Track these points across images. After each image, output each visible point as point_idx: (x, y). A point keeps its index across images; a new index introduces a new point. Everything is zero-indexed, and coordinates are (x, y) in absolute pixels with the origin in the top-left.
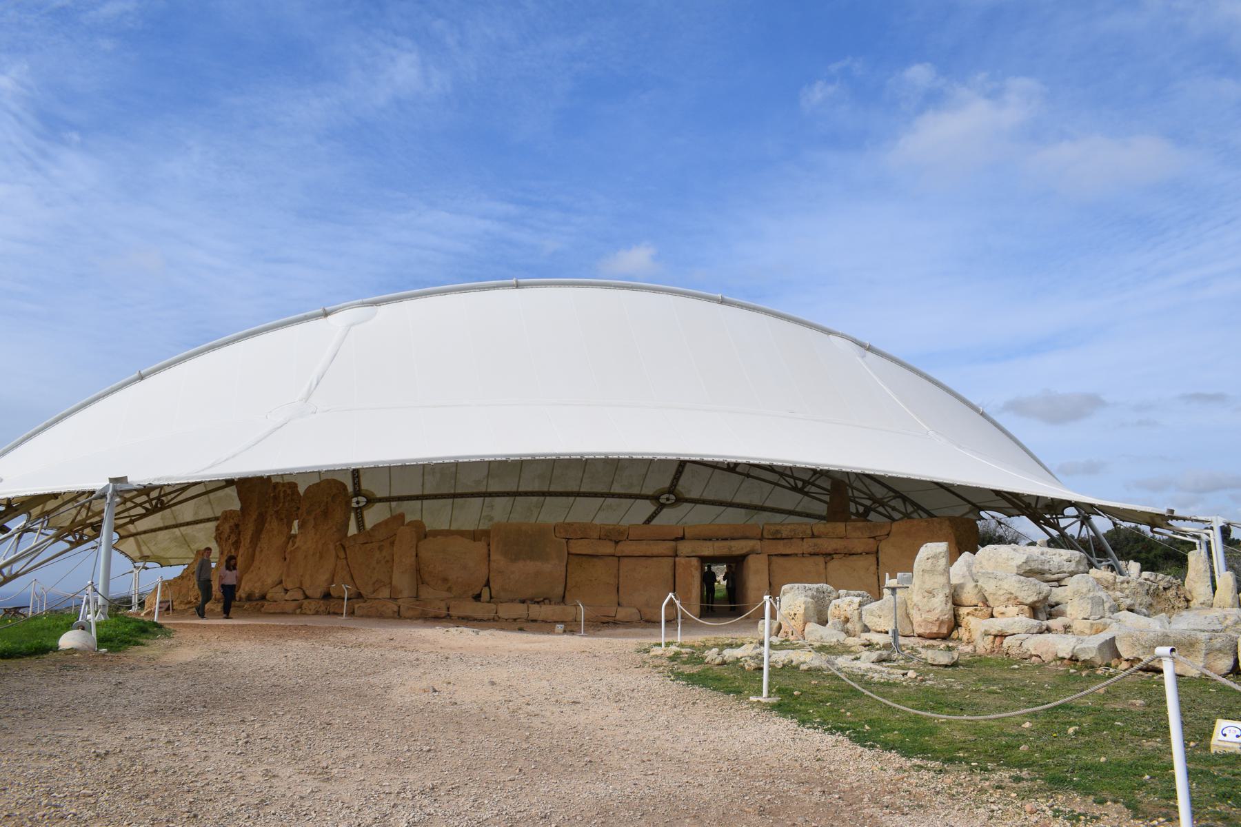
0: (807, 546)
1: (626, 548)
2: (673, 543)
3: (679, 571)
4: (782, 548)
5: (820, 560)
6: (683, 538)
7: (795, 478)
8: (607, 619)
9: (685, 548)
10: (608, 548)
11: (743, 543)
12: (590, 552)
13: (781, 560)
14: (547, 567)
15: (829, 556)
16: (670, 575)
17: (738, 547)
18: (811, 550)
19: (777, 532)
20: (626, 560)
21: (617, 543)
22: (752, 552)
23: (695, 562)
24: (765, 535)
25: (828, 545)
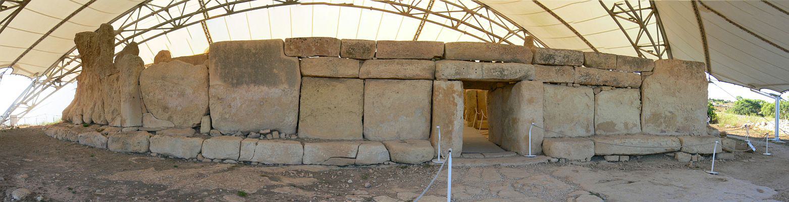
0: (578, 74)
1: (372, 68)
2: (432, 63)
3: (439, 97)
4: (553, 75)
5: (590, 91)
6: (443, 58)
7: (494, 36)
8: (343, 162)
9: (447, 68)
10: (350, 68)
11: (517, 66)
12: (328, 74)
13: (550, 89)
14: (274, 92)
15: (598, 87)
16: (427, 102)
17: (511, 70)
18: (582, 80)
19: (551, 57)
20: (373, 82)
21: (362, 61)
22: (526, 77)
23: (458, 86)
24: (537, 60)
25: (598, 75)
